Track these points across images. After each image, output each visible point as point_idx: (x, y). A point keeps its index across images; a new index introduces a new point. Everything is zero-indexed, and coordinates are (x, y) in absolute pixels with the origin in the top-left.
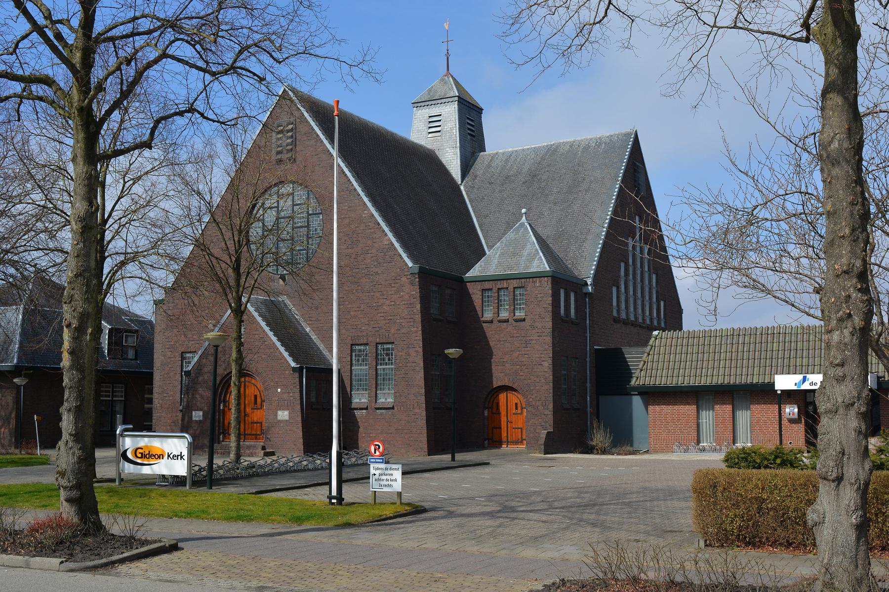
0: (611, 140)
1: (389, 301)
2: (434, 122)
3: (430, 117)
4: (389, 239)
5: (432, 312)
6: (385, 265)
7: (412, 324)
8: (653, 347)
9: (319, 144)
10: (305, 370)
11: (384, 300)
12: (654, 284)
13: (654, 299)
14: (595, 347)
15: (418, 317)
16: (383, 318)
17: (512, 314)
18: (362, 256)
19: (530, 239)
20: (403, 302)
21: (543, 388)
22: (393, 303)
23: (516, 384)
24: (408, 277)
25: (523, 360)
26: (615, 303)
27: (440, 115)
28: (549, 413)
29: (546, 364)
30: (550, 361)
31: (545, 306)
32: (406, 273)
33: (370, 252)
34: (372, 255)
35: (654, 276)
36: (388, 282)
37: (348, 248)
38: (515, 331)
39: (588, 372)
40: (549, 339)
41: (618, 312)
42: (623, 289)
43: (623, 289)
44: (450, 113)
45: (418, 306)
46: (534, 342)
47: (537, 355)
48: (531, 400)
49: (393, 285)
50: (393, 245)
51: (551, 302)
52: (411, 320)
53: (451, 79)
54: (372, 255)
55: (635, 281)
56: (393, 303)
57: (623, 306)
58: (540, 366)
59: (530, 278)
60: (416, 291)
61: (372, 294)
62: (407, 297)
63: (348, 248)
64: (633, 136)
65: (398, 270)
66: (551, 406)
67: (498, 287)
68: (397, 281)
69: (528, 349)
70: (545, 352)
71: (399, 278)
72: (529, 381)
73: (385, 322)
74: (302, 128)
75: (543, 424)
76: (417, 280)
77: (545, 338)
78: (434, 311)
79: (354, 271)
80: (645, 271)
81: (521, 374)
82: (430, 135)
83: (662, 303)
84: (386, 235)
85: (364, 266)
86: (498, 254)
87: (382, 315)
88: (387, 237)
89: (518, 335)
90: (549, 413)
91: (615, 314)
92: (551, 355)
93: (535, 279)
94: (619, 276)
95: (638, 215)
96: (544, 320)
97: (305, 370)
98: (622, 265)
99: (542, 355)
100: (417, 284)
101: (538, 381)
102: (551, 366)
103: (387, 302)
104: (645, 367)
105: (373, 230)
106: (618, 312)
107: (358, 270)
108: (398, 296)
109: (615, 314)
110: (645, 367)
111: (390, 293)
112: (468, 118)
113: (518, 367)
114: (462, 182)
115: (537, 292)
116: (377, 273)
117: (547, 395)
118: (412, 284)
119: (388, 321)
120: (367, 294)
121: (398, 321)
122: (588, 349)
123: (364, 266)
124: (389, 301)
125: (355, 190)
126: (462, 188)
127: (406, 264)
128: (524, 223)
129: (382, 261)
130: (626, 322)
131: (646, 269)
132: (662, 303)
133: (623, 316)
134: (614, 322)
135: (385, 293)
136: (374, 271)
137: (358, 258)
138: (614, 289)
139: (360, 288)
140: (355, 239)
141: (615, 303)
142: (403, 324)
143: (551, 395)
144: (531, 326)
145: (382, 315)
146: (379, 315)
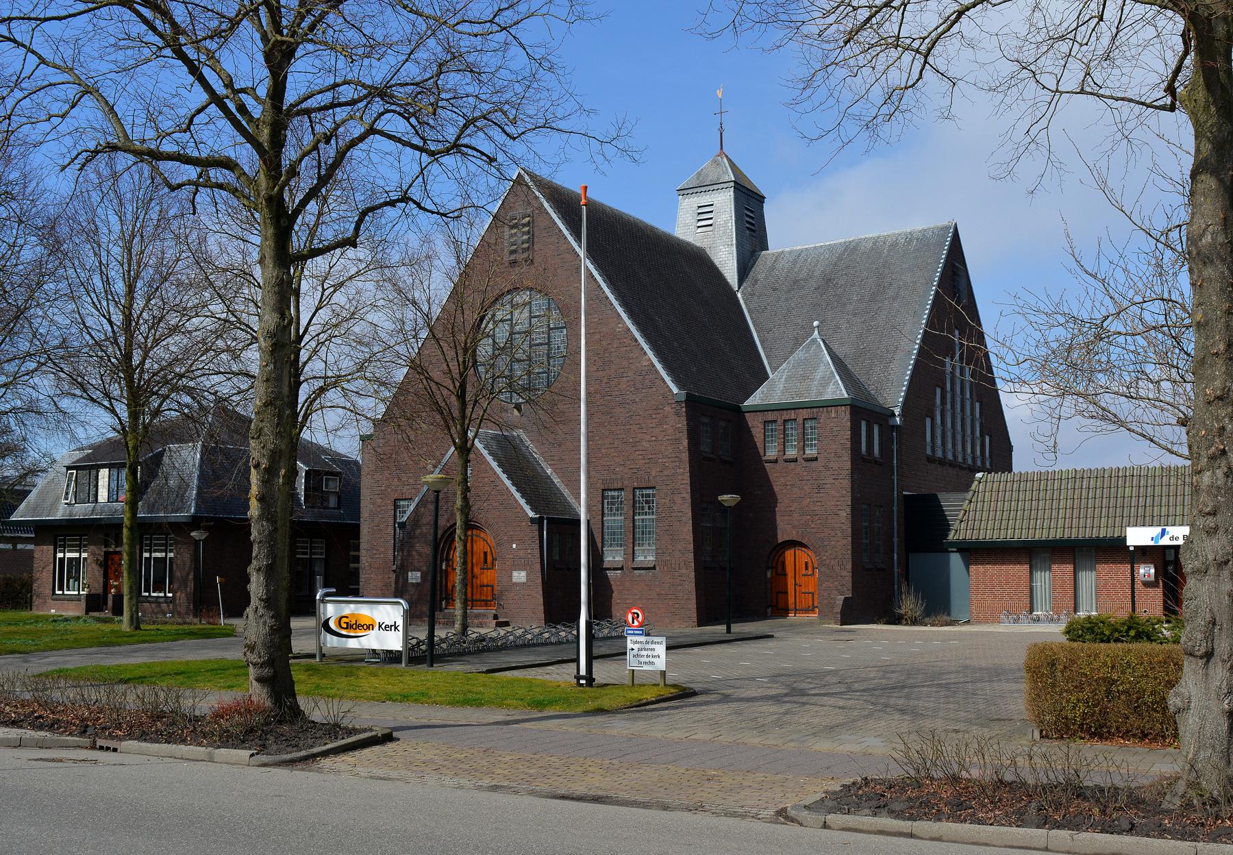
0: (924, 235)
1: (649, 436)
2: (704, 213)
3: (699, 207)
5: (702, 449)
6: (644, 391)
7: (678, 464)
9: (562, 241)
10: (545, 521)
14: (904, 493)
15: (685, 456)
16: (641, 457)
17: (802, 452)
18: (616, 380)
21: (839, 543)
22: (654, 439)
24: (673, 406)
25: (815, 508)
26: (928, 438)
27: (712, 205)
28: (847, 574)
29: (843, 514)
30: (849, 510)
31: (842, 441)
32: (670, 401)
33: (625, 375)
35: (978, 405)
36: (648, 412)
37: (598, 370)
38: (805, 473)
40: (847, 483)
44: (724, 202)
45: (685, 442)
46: (829, 486)
47: (833, 503)
48: (825, 558)
49: (654, 416)
51: (849, 437)
52: (677, 459)
53: (725, 159)
56: (654, 439)
57: (939, 442)
58: (835, 517)
59: (823, 407)
60: (682, 423)
62: (670, 431)
63: (598, 370)
64: (951, 230)
66: (849, 566)
69: (821, 495)
70: (843, 499)
71: (661, 407)
73: (644, 461)
74: (541, 222)
75: (839, 587)
76: (684, 409)
78: (705, 448)
79: (606, 398)
81: (812, 526)
82: (700, 230)
84: (645, 353)
85: (618, 393)
87: (640, 453)
91: (929, 452)
92: (850, 503)
93: (829, 409)
94: (934, 405)
97: (545, 521)
98: (938, 391)
99: (838, 503)
100: (684, 414)
102: (849, 516)
103: (647, 438)
105: (628, 348)
107: (610, 398)
109: (929, 452)
110: (966, 517)
111: (651, 425)
113: (808, 517)
114: (739, 288)
115: (832, 424)
116: (634, 402)
118: (678, 415)
120: (622, 427)
121: (660, 460)
122: (895, 495)
124: (649, 436)
125: (607, 298)
126: (739, 295)
127: (670, 390)
130: (942, 462)
134: (928, 461)
135: (644, 425)
138: (928, 421)
139: (613, 419)
140: (607, 359)
141: (928, 438)
143: (850, 552)
144: (825, 467)
145: (640, 453)
146: (637, 453)
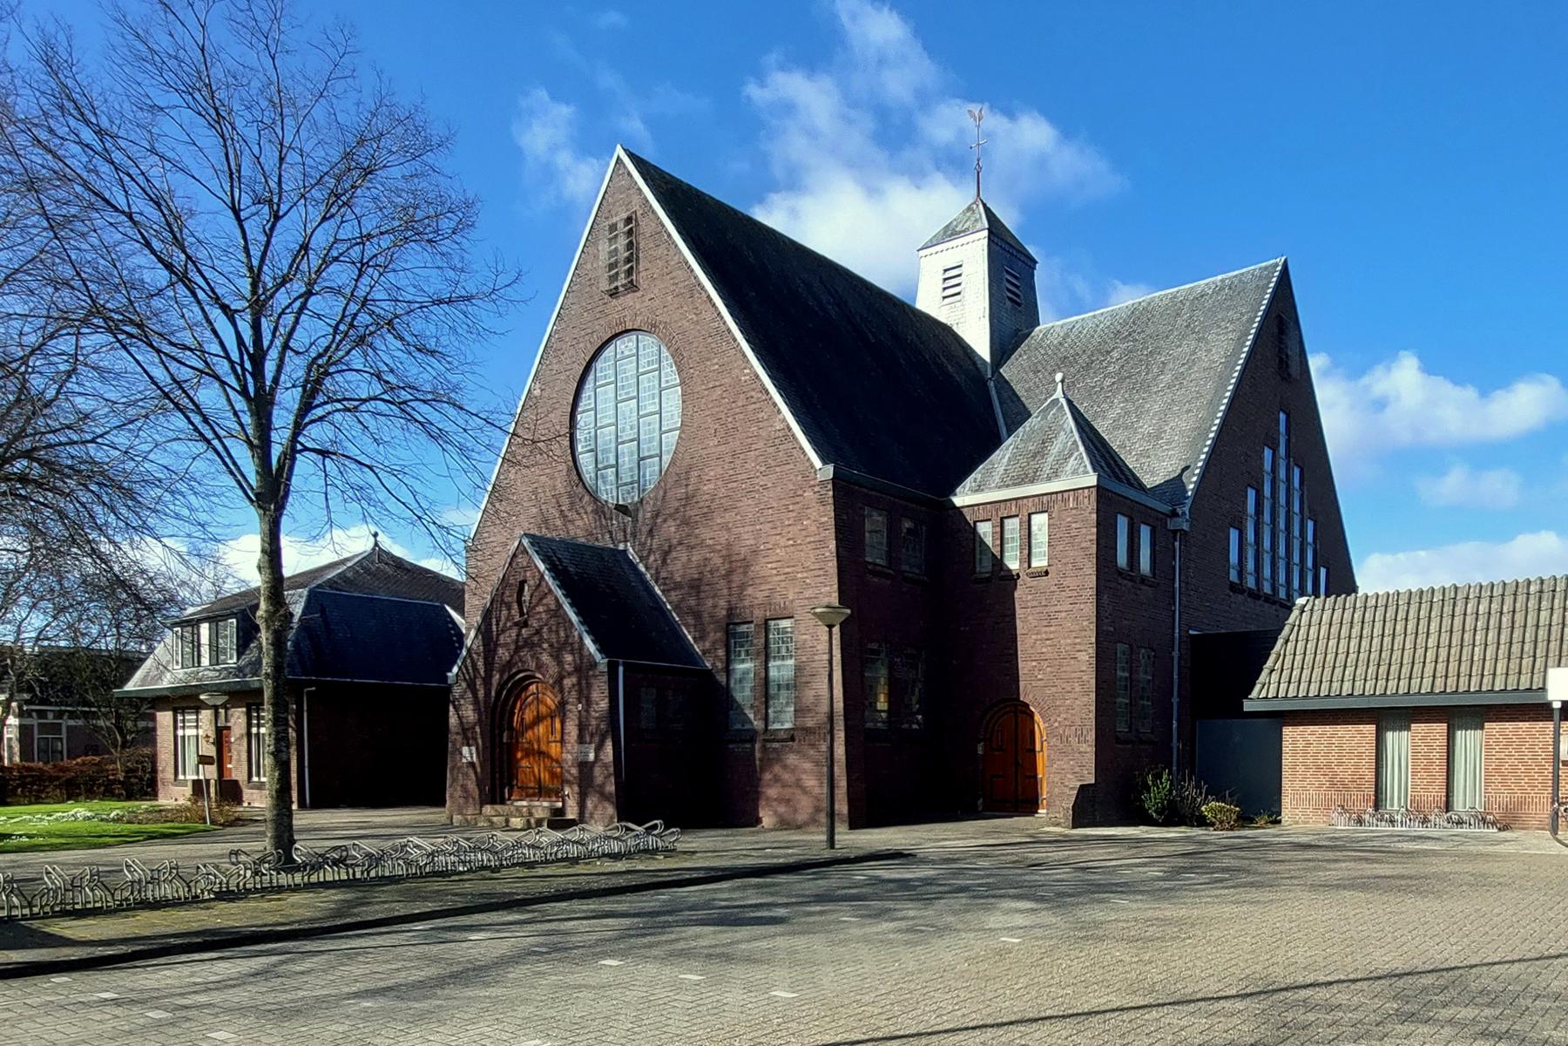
0: (1240, 281)
1: (784, 539)
2: (952, 279)
3: (945, 271)
4: (784, 420)
5: (868, 559)
6: (778, 469)
7: (821, 579)
8: (1296, 628)
9: (672, 252)
10: (621, 669)
11: (778, 537)
12: (1310, 538)
13: (1310, 564)
14: (1191, 632)
15: (832, 567)
16: (775, 572)
17: (1026, 565)
18: (742, 456)
19: (1065, 426)
20: (808, 540)
21: (1078, 702)
22: (791, 542)
23: (1031, 696)
24: (816, 489)
25: (1044, 650)
26: (1234, 558)
27: (960, 266)
28: (1088, 750)
29: (1084, 657)
30: (1092, 651)
31: (1084, 545)
32: (812, 483)
33: (754, 447)
34: (757, 453)
35: (1310, 524)
36: (784, 502)
37: (719, 444)
38: (1030, 597)
39: (1175, 677)
40: (1090, 609)
41: (1241, 573)
42: (1251, 536)
43: (1251, 536)
44: (973, 253)
45: (832, 545)
46: (1063, 614)
47: (1069, 641)
48: (1056, 724)
49: (791, 507)
50: (790, 429)
51: (1095, 537)
52: (821, 572)
53: (981, 207)
54: (757, 453)
55: (1274, 525)
56: (791, 542)
57: (1250, 566)
58: (1072, 662)
59: (1057, 493)
60: (827, 516)
61: (758, 527)
62: (813, 528)
63: (719, 444)
64: (1279, 268)
65: (799, 478)
66: (1092, 736)
67: (1000, 515)
68: (798, 499)
69: (1052, 629)
70: (1083, 634)
71: (800, 492)
72: (1054, 689)
73: (778, 578)
74: (646, 227)
75: (1077, 769)
76: (831, 493)
77: (1082, 606)
78: (875, 554)
79: (730, 486)
80: (1308, 544)
81: (1039, 677)
82: (947, 300)
83: (1323, 571)
84: (779, 412)
85: (745, 476)
86: (1007, 457)
87: (774, 565)
88: (781, 417)
89: (1035, 603)
90: (1089, 749)
91: (1233, 576)
92: (1094, 640)
93: (1066, 495)
94: (1245, 511)
95: (1284, 412)
96: (1081, 572)
97: (621, 669)
98: (1251, 494)
99: (1078, 640)
100: (831, 501)
101: (1069, 689)
102: (1093, 661)
103: (783, 542)
104: (1278, 665)
105: (757, 406)
106: (1241, 573)
107: (735, 485)
108: (799, 527)
109: (1233, 576)
110: (1278, 665)
111: (787, 523)
112: (1007, 272)
113: (1034, 664)
114: (993, 376)
115: (1069, 519)
116: (765, 487)
117: (1084, 716)
118: (822, 503)
119: (783, 577)
120: (751, 528)
121: (799, 575)
122: (1177, 635)
123: (745, 476)
124: (784, 539)
125: (729, 330)
126: (992, 384)
127: (812, 466)
128: (1058, 399)
129: (773, 464)
130: (1255, 595)
131: (1296, 508)
132: (1323, 571)
133: (1251, 582)
134: (1231, 590)
135: (778, 523)
136: (761, 483)
137: (737, 462)
138: (1234, 535)
139: (738, 517)
140: (730, 426)
141: (1234, 558)
142: (808, 581)
143: (1092, 715)
144: (1059, 585)
145: (774, 565)
146: (770, 566)
